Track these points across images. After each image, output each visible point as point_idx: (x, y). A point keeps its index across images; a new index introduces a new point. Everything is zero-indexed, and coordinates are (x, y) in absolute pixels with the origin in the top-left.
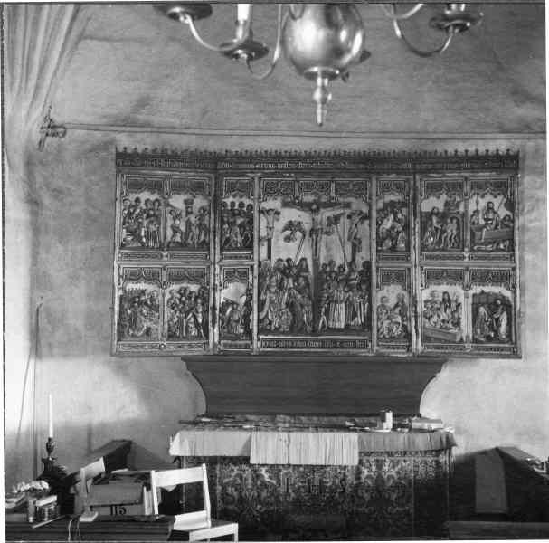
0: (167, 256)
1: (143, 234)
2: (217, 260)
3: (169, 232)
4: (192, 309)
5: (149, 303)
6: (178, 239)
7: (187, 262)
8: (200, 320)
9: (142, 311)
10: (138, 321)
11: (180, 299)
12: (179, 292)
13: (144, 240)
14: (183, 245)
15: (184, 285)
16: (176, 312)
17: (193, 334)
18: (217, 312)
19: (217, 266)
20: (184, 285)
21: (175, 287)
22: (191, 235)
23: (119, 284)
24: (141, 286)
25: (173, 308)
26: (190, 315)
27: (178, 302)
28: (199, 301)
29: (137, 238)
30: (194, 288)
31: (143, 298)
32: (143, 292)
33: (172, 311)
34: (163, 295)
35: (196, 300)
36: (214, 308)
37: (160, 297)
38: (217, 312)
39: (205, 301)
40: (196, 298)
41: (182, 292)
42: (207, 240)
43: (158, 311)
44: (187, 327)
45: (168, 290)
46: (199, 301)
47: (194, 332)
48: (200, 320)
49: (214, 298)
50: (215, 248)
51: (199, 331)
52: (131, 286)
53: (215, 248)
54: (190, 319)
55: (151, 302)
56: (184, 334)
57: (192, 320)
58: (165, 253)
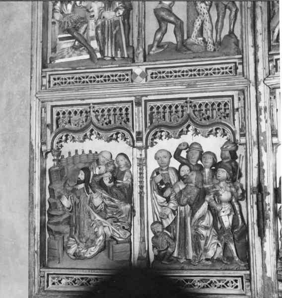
0: (144, 75)
1: (92, 33)
2: (261, 77)
3: (152, 25)
4: (203, 193)
5: (106, 182)
6: (170, 37)
7: (189, 86)
8: (227, 221)
9: (90, 201)
10: (85, 222)
11: (178, 172)
12: (177, 155)
13: (94, 44)
14: (182, 48)
15: (189, 138)
16: (168, 200)
17: (210, 254)
18: (269, 200)
19: (261, 88)
20: (189, 138)
21: (169, 144)
22: (198, 24)
23: (44, 143)
24: (95, 145)
25: (161, 192)
26: (205, 206)
27: (173, 178)
28: (223, 174)
29: (83, 44)
30: (213, 144)
31: (97, 171)
32: (95, 158)
33: (161, 199)
34: (142, 163)
35: (214, 172)
36: (260, 189)
37: (135, 170)
38: (269, 200)
39: (235, 175)
40: (216, 166)
41: (184, 154)
42: (237, 32)
43: (129, 199)
44: (197, 237)
45: (152, 152)
46: (223, 174)
47: (214, 250)
48: (227, 221)
49: (260, 165)
50: (255, 46)
51: (225, 247)
52: (69, 148)
53: (255, 46)
54: (202, 217)
55: (114, 179)
56: (191, 254)
57: (209, 219)
58: (138, 70)
